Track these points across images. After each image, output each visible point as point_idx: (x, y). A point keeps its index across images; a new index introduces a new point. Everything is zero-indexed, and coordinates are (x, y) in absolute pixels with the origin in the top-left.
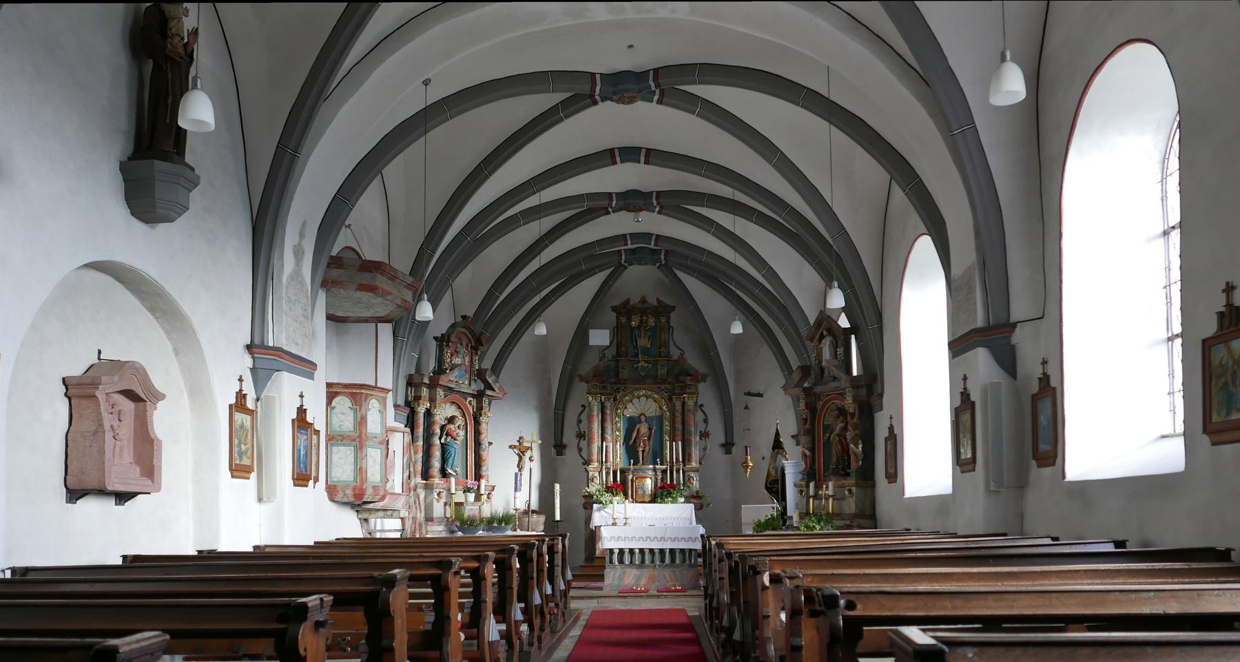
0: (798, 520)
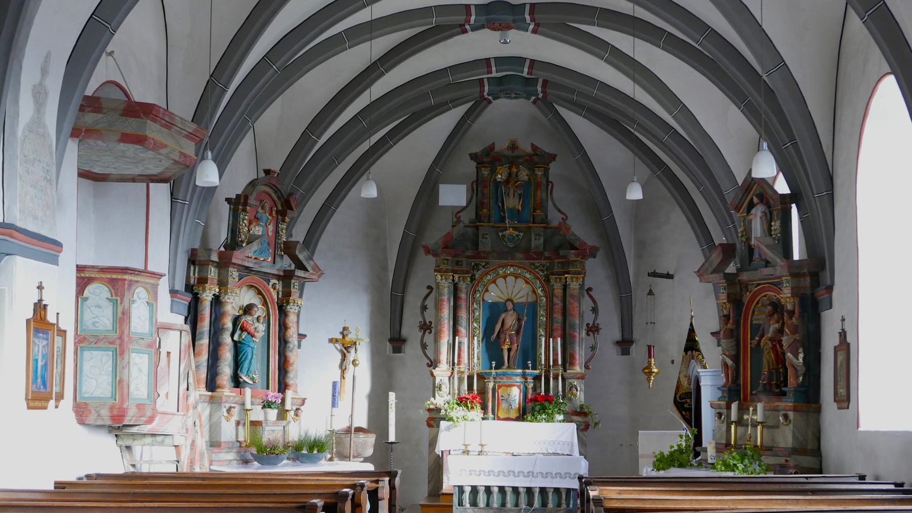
0: (714, 454)
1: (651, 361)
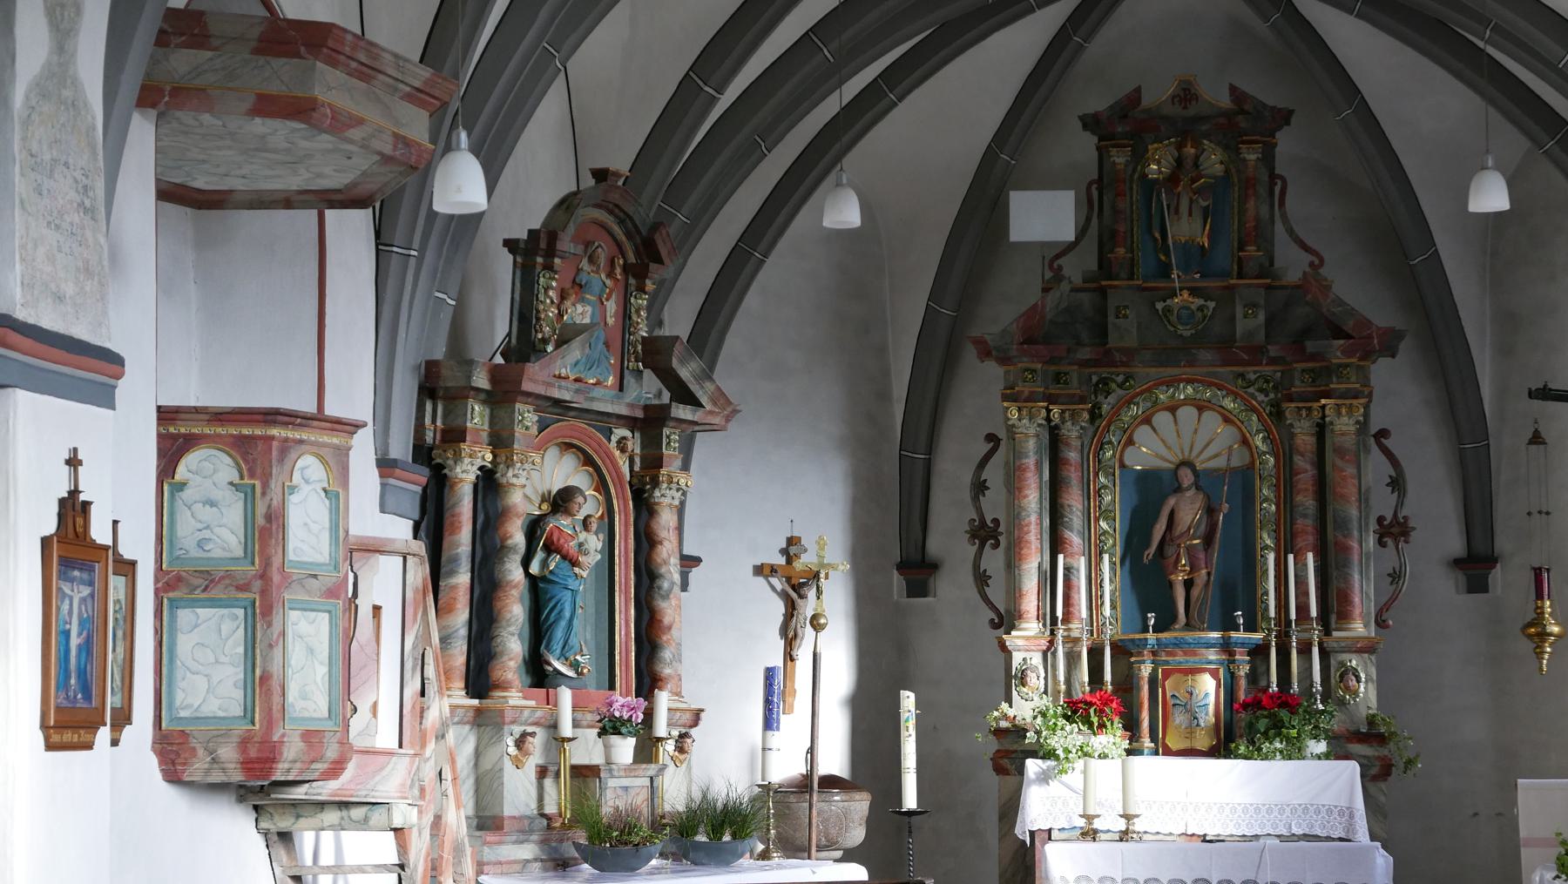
1: (1542, 607)
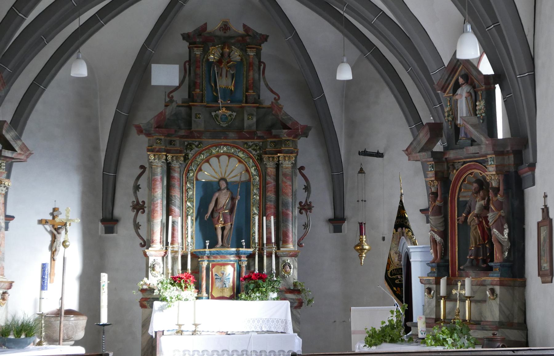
0: (425, 329)
1: (362, 239)
